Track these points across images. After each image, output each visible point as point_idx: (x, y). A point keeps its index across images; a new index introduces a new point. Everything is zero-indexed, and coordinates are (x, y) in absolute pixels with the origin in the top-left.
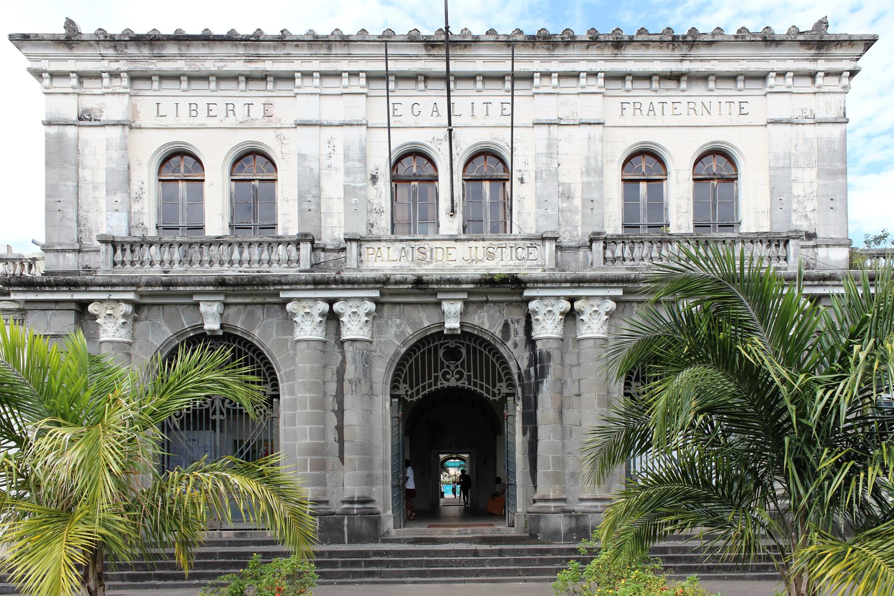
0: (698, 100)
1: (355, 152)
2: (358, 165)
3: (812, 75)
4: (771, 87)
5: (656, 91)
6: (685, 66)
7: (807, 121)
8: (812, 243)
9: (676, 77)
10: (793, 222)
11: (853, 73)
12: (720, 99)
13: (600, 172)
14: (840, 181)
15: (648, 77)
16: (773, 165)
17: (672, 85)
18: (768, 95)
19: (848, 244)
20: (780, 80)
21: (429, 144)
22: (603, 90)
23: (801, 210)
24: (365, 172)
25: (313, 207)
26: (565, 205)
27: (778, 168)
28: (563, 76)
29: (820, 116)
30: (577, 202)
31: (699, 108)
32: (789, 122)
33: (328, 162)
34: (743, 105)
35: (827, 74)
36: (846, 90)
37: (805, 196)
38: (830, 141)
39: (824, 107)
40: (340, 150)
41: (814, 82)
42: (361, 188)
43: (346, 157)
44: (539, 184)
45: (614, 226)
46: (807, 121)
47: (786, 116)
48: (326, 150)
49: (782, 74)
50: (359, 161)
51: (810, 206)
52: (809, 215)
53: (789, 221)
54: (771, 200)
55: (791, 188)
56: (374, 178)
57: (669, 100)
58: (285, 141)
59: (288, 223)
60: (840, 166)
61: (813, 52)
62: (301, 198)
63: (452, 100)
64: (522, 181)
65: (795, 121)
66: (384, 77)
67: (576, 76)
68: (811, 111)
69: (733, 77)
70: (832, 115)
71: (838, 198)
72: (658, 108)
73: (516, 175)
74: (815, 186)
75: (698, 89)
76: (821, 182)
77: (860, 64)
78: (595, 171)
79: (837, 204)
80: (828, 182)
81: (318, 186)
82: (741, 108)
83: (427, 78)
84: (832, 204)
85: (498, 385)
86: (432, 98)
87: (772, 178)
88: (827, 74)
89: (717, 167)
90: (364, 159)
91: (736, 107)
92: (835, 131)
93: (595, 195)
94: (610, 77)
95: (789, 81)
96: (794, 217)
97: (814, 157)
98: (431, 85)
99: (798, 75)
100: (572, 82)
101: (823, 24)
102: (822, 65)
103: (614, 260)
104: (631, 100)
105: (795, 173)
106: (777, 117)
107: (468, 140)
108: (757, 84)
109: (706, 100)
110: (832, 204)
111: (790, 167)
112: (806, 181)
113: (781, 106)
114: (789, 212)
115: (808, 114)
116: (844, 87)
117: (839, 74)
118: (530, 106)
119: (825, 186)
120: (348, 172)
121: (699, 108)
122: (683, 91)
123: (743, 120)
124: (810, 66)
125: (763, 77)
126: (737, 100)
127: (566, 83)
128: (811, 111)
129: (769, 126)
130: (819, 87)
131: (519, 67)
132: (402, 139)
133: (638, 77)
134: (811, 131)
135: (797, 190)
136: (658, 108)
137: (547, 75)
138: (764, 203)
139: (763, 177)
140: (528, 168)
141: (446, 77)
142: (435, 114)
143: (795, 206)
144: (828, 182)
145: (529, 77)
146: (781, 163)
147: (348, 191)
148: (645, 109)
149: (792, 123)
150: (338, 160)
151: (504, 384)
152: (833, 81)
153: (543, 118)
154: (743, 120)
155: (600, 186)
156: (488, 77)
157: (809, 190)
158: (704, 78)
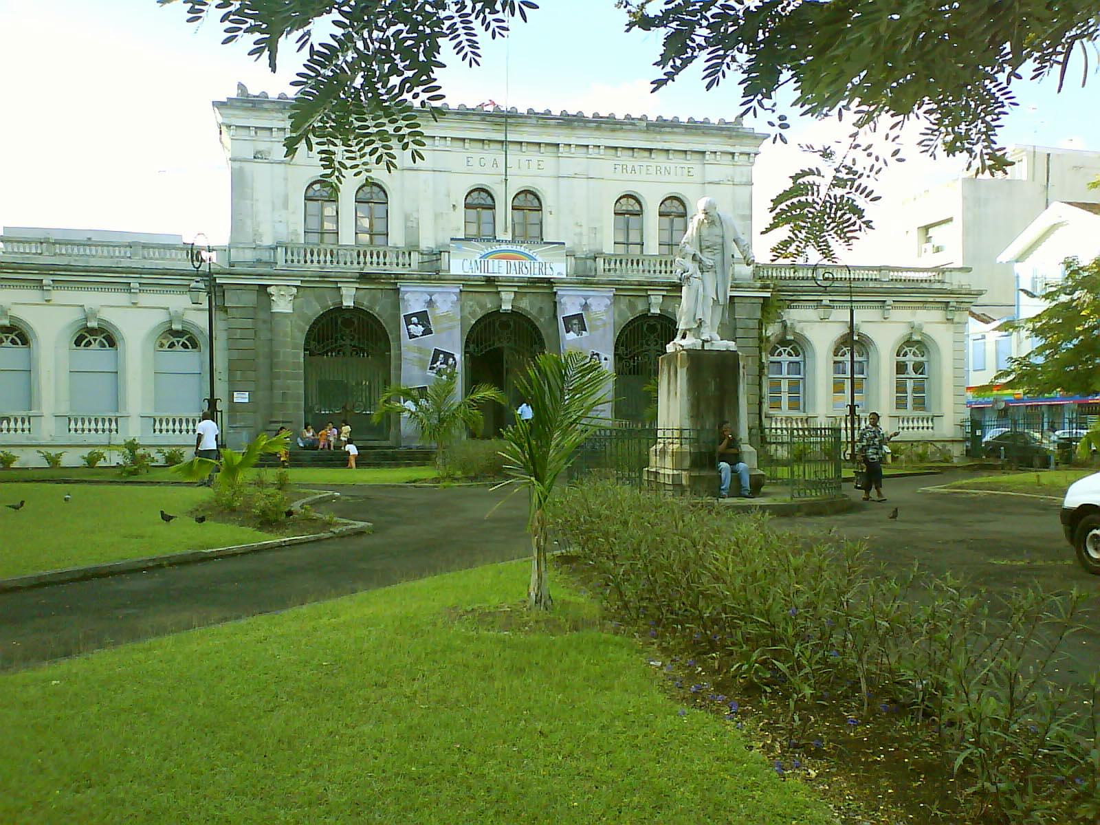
3: (733, 154)
11: (756, 154)
12: (676, 165)
25: (415, 225)
29: (737, 180)
30: (585, 230)
31: (663, 171)
36: (753, 164)
39: (739, 174)
41: (733, 158)
57: (645, 164)
59: (397, 237)
64: (551, 213)
70: (744, 180)
77: (760, 149)
86: (494, 154)
88: (741, 154)
89: (675, 209)
91: (686, 170)
92: (744, 190)
107: (515, 186)
109: (668, 166)
121: (663, 171)
124: (731, 149)
126: (686, 166)
136: (637, 168)
142: (495, 166)
148: (629, 170)
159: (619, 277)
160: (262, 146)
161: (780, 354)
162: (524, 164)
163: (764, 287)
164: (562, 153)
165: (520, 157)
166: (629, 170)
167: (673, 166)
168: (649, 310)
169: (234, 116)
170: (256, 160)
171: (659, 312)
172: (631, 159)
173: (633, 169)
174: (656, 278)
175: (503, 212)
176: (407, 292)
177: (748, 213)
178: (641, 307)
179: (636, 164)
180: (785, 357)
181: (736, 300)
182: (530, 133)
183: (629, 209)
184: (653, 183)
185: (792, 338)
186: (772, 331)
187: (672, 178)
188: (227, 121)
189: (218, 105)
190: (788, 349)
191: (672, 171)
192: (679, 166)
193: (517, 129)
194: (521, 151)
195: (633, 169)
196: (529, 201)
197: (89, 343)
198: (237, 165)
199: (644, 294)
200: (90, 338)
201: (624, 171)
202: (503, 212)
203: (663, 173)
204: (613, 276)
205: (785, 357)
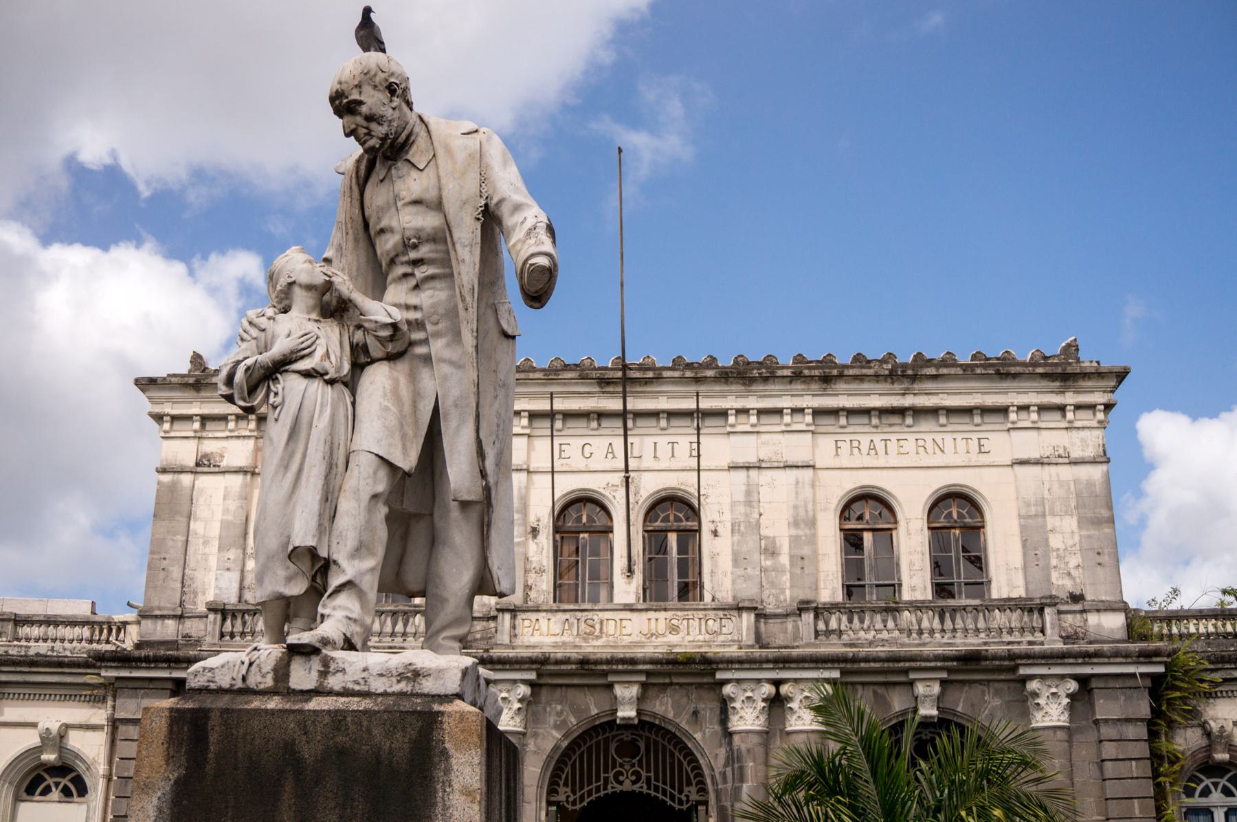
0: (928, 437)
3: (1062, 409)
4: (1013, 423)
5: (876, 427)
6: (908, 401)
7: (1060, 460)
8: (1078, 607)
9: (901, 412)
10: (1054, 580)
11: (1108, 407)
12: (955, 435)
13: (812, 523)
14: (1107, 530)
15: (867, 412)
16: (1023, 512)
17: (896, 419)
18: (1013, 433)
19: (1124, 608)
20: (1023, 415)
21: (602, 491)
22: (812, 428)
23: (1063, 566)
26: (769, 563)
27: (1030, 517)
28: (761, 412)
29: (1076, 454)
30: (784, 559)
31: (929, 445)
32: (1039, 462)
34: (982, 442)
35: (1078, 407)
37: (1066, 549)
38: (1090, 484)
41: (1064, 416)
44: (736, 538)
45: (830, 589)
46: (1060, 460)
47: (1035, 455)
49: (1024, 408)
51: (1074, 561)
52: (1074, 572)
53: (1048, 579)
54: (1025, 555)
55: (1047, 540)
56: (535, 532)
57: (894, 437)
60: (1105, 513)
61: (1058, 384)
63: (630, 440)
64: (715, 533)
65: (1046, 460)
66: (551, 415)
67: (779, 412)
68: (1065, 448)
69: (968, 411)
70: (1090, 453)
71: (1106, 551)
72: (880, 446)
74: (1077, 538)
75: (926, 425)
76: (1084, 533)
78: (805, 522)
79: (1105, 559)
80: (1092, 532)
82: (980, 446)
83: (601, 415)
84: (1099, 559)
85: (686, 789)
87: (1023, 529)
88: (1078, 407)
93: (806, 551)
94: (818, 413)
95: (1034, 416)
96: (1054, 575)
97: (1073, 504)
98: (605, 423)
99: (1042, 408)
100: (775, 419)
101: (1071, 349)
102: (1070, 398)
103: (828, 633)
104: (848, 438)
105: (1051, 522)
106: (1024, 456)
107: (649, 486)
108: (998, 418)
109: (938, 438)
110: (1099, 559)
111: (1044, 516)
112: (1065, 532)
113: (1029, 444)
114: (1047, 569)
115: (1061, 452)
116: (1100, 422)
117: (1092, 407)
118: (719, 447)
119: (1089, 537)
121: (929, 445)
122: (909, 426)
123: (984, 459)
125: (1003, 411)
126: (975, 436)
128: (1065, 448)
129: (1016, 467)
130: (1070, 422)
131: (705, 404)
132: (567, 485)
133: (851, 412)
134: (1066, 472)
135: (1055, 542)
136: (880, 446)
137: (744, 412)
138: (1017, 560)
139: (1014, 526)
140: (722, 518)
141: (623, 415)
142: (610, 456)
143: (1054, 562)
144: (1092, 532)
145: (723, 414)
146: (1033, 510)
149: (1042, 464)
151: (693, 789)
152: (1087, 414)
153: (741, 460)
154: (984, 459)
155: (812, 540)
156: (672, 414)
157: (1070, 542)
158: (934, 412)
159: (845, 645)
160: (209, 447)
161: (1206, 793)
163: (1147, 656)
165: (655, 439)
167: (948, 438)
168: (915, 710)
169: (169, 399)
170: (199, 469)
171: (935, 712)
172: (866, 429)
174: (924, 645)
175: (625, 540)
177: (1105, 513)
179: (877, 439)
180: (1216, 797)
181: (1094, 684)
183: (866, 514)
184: (911, 468)
185: (1226, 756)
186: (1187, 741)
188: (158, 409)
189: (147, 384)
190: (1223, 782)
192: (959, 436)
193: (648, 389)
196: (674, 515)
197: (47, 791)
198: (166, 478)
199: (902, 679)
200: (50, 781)
202: (625, 540)
203: (930, 450)
204: (833, 647)
205: (1216, 797)
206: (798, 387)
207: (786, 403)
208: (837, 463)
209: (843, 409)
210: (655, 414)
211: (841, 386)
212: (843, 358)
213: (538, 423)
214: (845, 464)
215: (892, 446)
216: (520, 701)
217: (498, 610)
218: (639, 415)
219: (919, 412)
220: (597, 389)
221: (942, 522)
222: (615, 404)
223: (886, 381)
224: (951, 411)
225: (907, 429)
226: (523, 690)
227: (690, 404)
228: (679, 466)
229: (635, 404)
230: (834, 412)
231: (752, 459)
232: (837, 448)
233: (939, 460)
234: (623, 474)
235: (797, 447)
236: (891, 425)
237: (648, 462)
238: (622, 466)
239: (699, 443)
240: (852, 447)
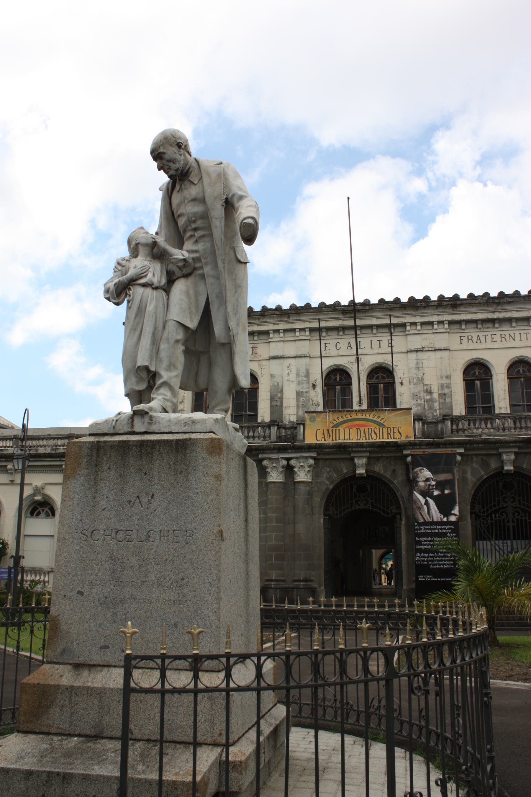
0: (507, 333)
1: (303, 372)
2: (305, 379)
5: (480, 329)
6: (496, 315)
9: (492, 321)
12: (521, 332)
15: (475, 322)
17: (490, 325)
21: (346, 365)
22: (448, 330)
24: (308, 383)
25: (279, 404)
28: (422, 324)
30: (436, 396)
31: (507, 337)
33: (287, 378)
40: (294, 371)
42: (306, 392)
43: (298, 375)
48: (287, 371)
50: (305, 377)
56: (314, 386)
57: (489, 334)
58: (263, 367)
62: (272, 399)
63: (359, 340)
64: (402, 384)
73: (397, 381)
81: (282, 391)
83: (344, 328)
90: (308, 375)
93: (446, 391)
94: (451, 323)
100: (430, 327)
103: (458, 431)
104: (466, 335)
107: (368, 362)
109: (512, 333)
120: (299, 383)
121: (507, 337)
122: (497, 328)
127: (425, 327)
131: (394, 321)
133: (467, 322)
136: (482, 339)
137: (414, 324)
141: (355, 328)
145: (404, 325)
147: (299, 394)
148: (475, 339)
150: (293, 377)
153: (413, 347)
156: (379, 327)
158: (509, 320)
159: (467, 436)
162: (375, 344)
164: (409, 331)
166: (475, 339)
167: (517, 333)
171: (512, 468)
172: (475, 330)
173: (479, 339)
174: (506, 435)
176: (264, 459)
178: (494, 465)
179: (481, 334)
182: (378, 317)
187: (518, 343)
191: (517, 337)
194: (372, 333)
195: (479, 339)
199: (495, 452)
201: (470, 341)
203: (508, 339)
206: (440, 310)
207: (435, 318)
208: (461, 347)
209: (464, 321)
210: (370, 327)
211: (462, 309)
212: (463, 296)
213: (314, 334)
214: (465, 348)
215: (489, 338)
216: (309, 466)
217: (298, 424)
218: (363, 327)
219: (502, 321)
220: (342, 316)
221: (515, 375)
222: (351, 323)
223: (484, 305)
224: (518, 320)
225: (495, 330)
226: (312, 462)
227: (386, 321)
228: (383, 351)
229: (359, 322)
230: (459, 322)
231: (419, 347)
232: (461, 340)
233: (512, 344)
234: (356, 356)
235: (441, 340)
236: (488, 328)
237: (368, 350)
238: (355, 352)
239: (391, 340)
240: (468, 339)
